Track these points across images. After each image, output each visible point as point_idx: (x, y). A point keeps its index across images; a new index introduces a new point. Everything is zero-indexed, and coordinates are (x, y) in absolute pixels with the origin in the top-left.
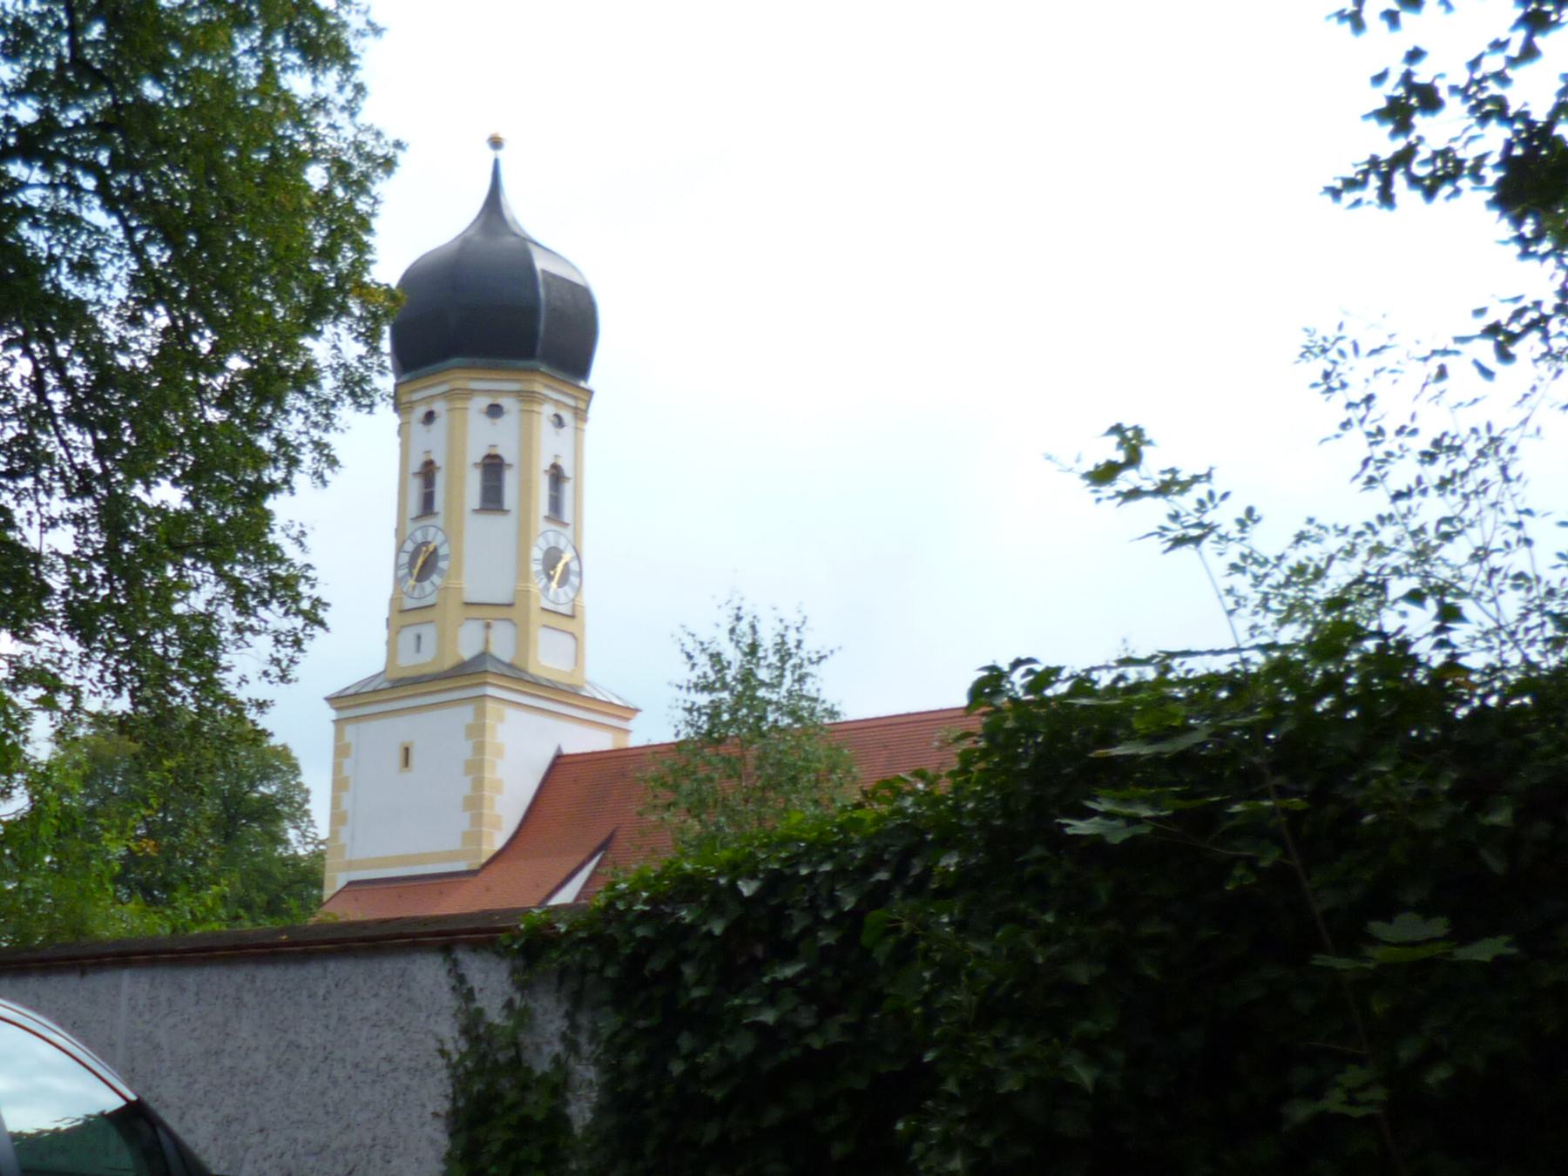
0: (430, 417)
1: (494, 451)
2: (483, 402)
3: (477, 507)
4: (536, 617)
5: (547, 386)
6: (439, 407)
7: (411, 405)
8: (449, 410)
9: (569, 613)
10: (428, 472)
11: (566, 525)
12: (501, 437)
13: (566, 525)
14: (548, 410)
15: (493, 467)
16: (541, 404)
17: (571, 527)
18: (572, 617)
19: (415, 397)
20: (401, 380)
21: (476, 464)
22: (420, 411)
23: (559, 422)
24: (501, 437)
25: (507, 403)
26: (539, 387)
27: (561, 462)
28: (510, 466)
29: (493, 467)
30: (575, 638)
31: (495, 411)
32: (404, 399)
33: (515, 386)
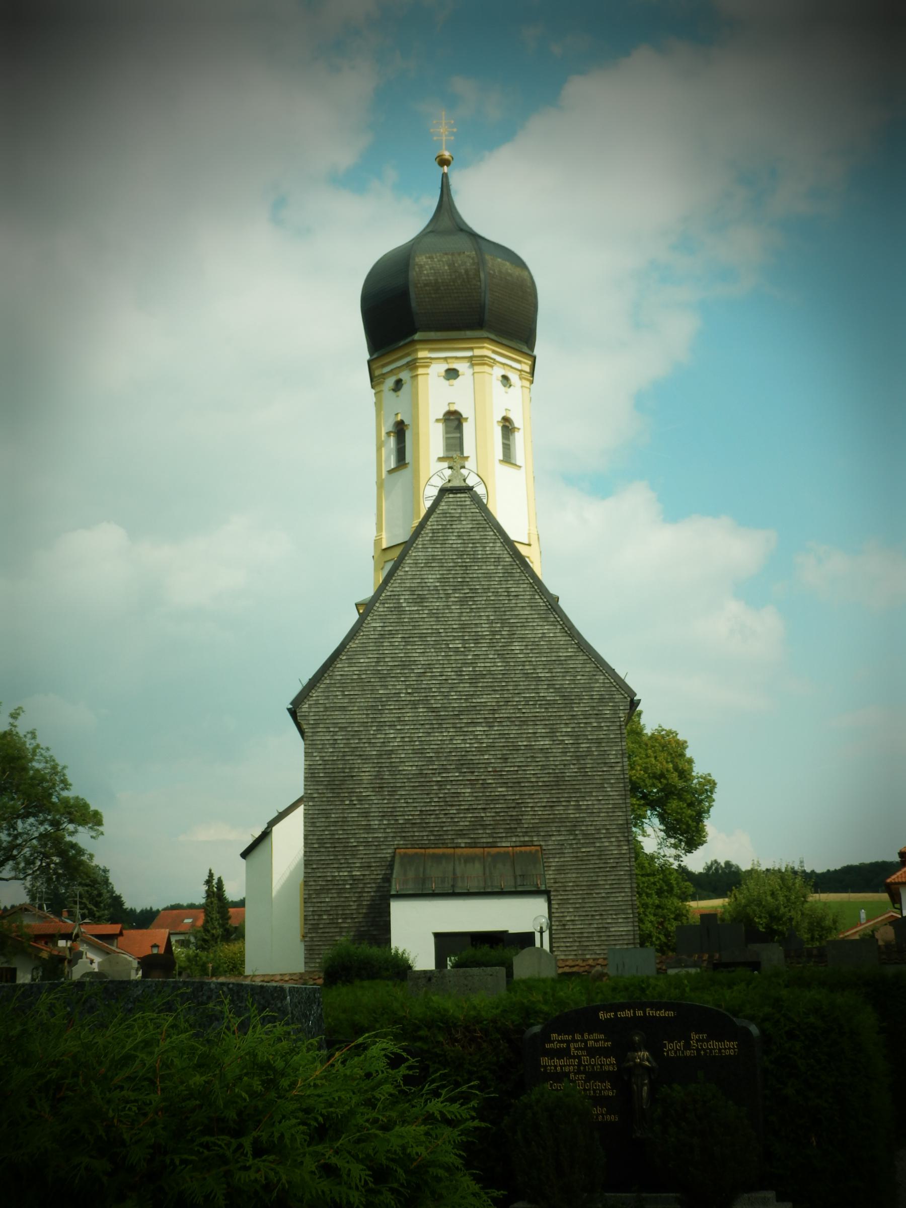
0: (399, 384)
1: (453, 408)
2: (442, 367)
3: (441, 455)
5: (494, 352)
6: (404, 375)
7: (384, 376)
8: (412, 377)
9: (527, 542)
10: (400, 430)
14: (498, 371)
17: (523, 469)
18: (529, 545)
19: (386, 370)
20: (375, 356)
21: (437, 420)
22: (390, 382)
25: (462, 367)
26: (486, 350)
28: (466, 419)
31: (452, 374)
32: (377, 373)
33: (468, 354)
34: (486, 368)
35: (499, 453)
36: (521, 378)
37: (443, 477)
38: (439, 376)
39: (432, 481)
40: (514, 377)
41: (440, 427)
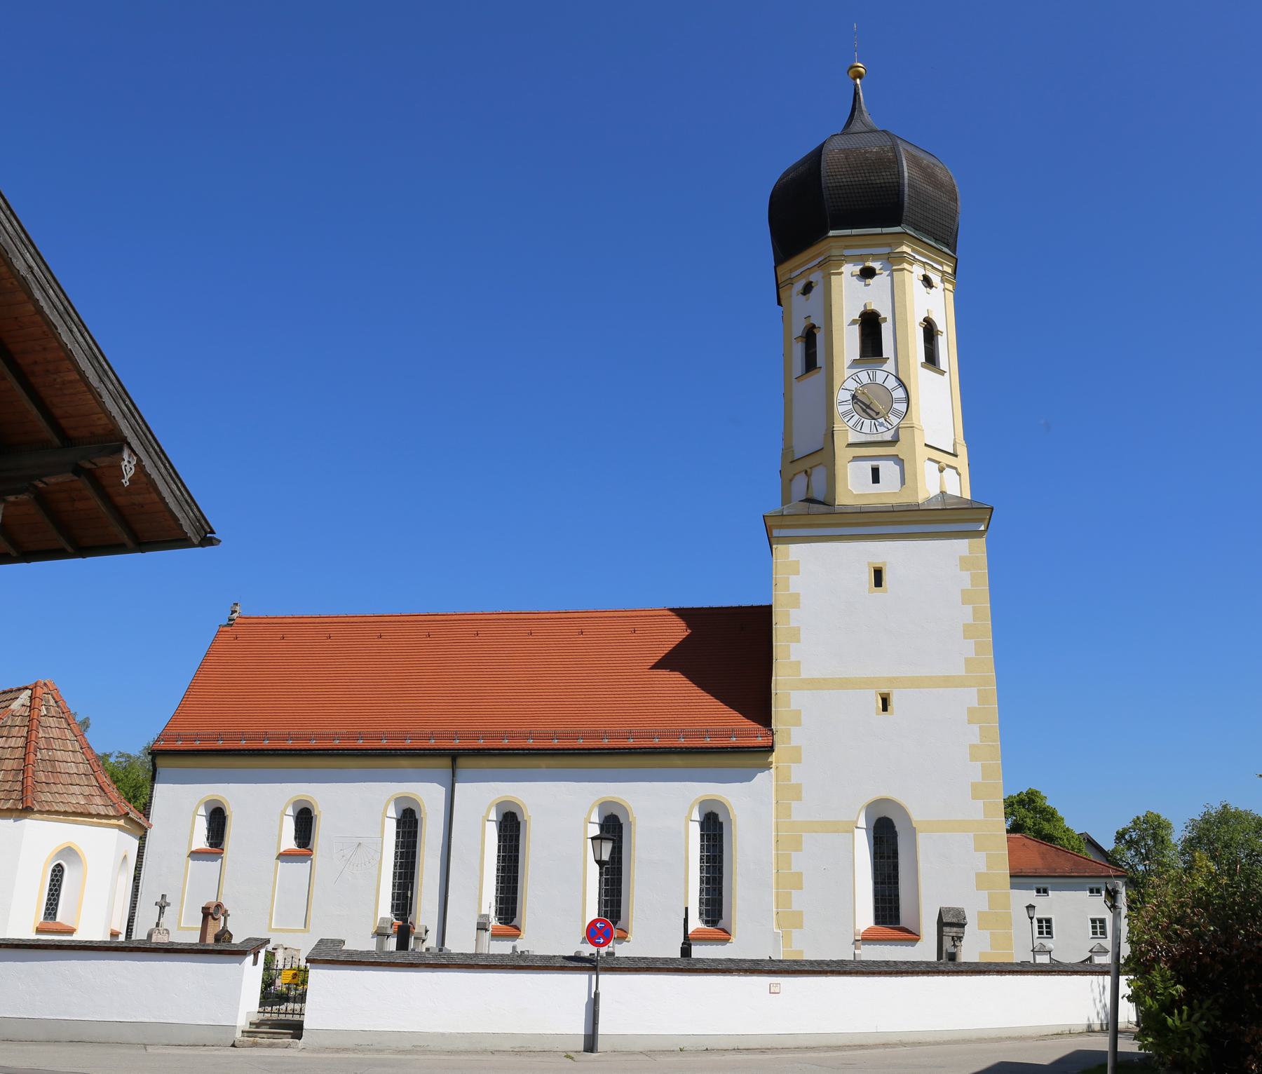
0: (808, 289)
4: (922, 453)
6: (815, 277)
7: (791, 282)
10: (810, 336)
11: (942, 373)
12: (875, 296)
13: (942, 373)
14: (918, 271)
15: (870, 324)
16: (912, 264)
17: (947, 375)
18: (955, 455)
21: (854, 322)
22: (799, 285)
23: (927, 282)
24: (875, 296)
27: (934, 317)
29: (870, 324)
30: (959, 474)
31: (868, 273)
33: (886, 250)
34: (906, 266)
35: (921, 357)
36: (942, 281)
37: (858, 380)
38: (852, 276)
39: (846, 385)
40: (936, 278)
41: (856, 329)
